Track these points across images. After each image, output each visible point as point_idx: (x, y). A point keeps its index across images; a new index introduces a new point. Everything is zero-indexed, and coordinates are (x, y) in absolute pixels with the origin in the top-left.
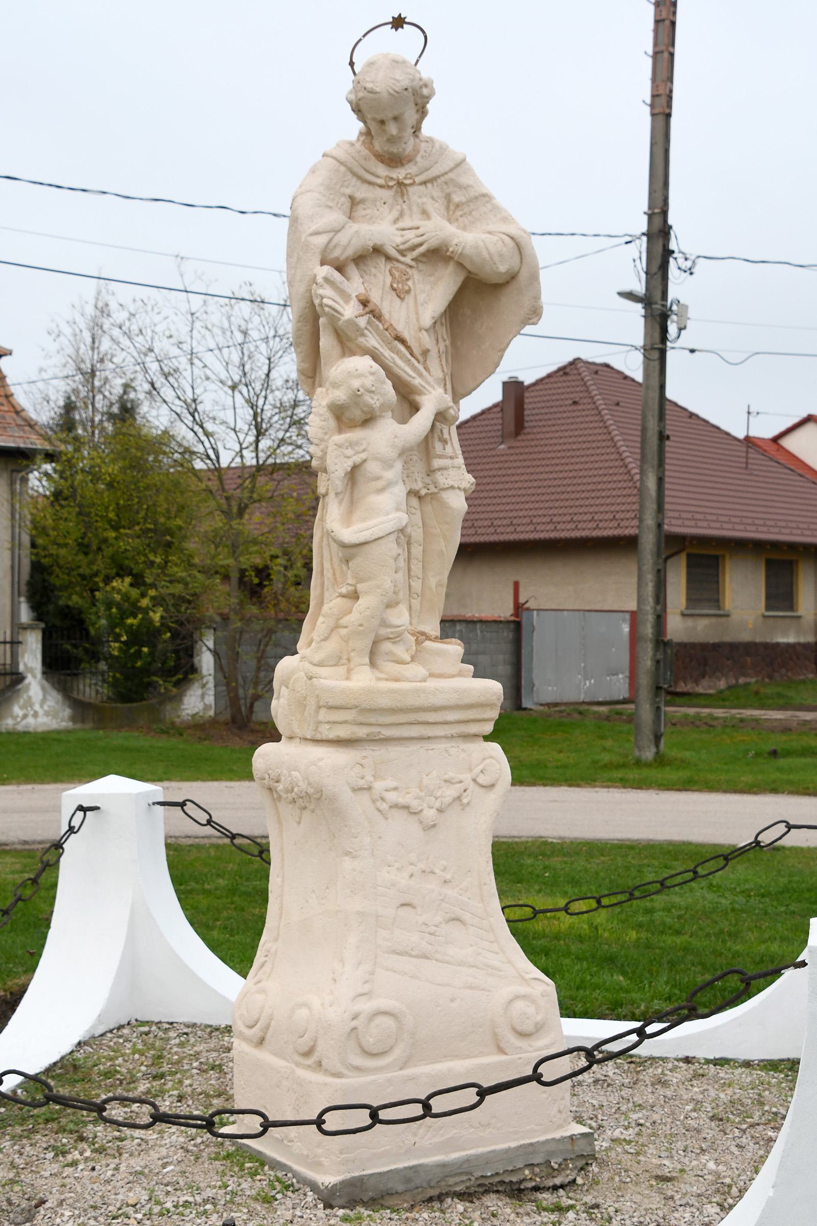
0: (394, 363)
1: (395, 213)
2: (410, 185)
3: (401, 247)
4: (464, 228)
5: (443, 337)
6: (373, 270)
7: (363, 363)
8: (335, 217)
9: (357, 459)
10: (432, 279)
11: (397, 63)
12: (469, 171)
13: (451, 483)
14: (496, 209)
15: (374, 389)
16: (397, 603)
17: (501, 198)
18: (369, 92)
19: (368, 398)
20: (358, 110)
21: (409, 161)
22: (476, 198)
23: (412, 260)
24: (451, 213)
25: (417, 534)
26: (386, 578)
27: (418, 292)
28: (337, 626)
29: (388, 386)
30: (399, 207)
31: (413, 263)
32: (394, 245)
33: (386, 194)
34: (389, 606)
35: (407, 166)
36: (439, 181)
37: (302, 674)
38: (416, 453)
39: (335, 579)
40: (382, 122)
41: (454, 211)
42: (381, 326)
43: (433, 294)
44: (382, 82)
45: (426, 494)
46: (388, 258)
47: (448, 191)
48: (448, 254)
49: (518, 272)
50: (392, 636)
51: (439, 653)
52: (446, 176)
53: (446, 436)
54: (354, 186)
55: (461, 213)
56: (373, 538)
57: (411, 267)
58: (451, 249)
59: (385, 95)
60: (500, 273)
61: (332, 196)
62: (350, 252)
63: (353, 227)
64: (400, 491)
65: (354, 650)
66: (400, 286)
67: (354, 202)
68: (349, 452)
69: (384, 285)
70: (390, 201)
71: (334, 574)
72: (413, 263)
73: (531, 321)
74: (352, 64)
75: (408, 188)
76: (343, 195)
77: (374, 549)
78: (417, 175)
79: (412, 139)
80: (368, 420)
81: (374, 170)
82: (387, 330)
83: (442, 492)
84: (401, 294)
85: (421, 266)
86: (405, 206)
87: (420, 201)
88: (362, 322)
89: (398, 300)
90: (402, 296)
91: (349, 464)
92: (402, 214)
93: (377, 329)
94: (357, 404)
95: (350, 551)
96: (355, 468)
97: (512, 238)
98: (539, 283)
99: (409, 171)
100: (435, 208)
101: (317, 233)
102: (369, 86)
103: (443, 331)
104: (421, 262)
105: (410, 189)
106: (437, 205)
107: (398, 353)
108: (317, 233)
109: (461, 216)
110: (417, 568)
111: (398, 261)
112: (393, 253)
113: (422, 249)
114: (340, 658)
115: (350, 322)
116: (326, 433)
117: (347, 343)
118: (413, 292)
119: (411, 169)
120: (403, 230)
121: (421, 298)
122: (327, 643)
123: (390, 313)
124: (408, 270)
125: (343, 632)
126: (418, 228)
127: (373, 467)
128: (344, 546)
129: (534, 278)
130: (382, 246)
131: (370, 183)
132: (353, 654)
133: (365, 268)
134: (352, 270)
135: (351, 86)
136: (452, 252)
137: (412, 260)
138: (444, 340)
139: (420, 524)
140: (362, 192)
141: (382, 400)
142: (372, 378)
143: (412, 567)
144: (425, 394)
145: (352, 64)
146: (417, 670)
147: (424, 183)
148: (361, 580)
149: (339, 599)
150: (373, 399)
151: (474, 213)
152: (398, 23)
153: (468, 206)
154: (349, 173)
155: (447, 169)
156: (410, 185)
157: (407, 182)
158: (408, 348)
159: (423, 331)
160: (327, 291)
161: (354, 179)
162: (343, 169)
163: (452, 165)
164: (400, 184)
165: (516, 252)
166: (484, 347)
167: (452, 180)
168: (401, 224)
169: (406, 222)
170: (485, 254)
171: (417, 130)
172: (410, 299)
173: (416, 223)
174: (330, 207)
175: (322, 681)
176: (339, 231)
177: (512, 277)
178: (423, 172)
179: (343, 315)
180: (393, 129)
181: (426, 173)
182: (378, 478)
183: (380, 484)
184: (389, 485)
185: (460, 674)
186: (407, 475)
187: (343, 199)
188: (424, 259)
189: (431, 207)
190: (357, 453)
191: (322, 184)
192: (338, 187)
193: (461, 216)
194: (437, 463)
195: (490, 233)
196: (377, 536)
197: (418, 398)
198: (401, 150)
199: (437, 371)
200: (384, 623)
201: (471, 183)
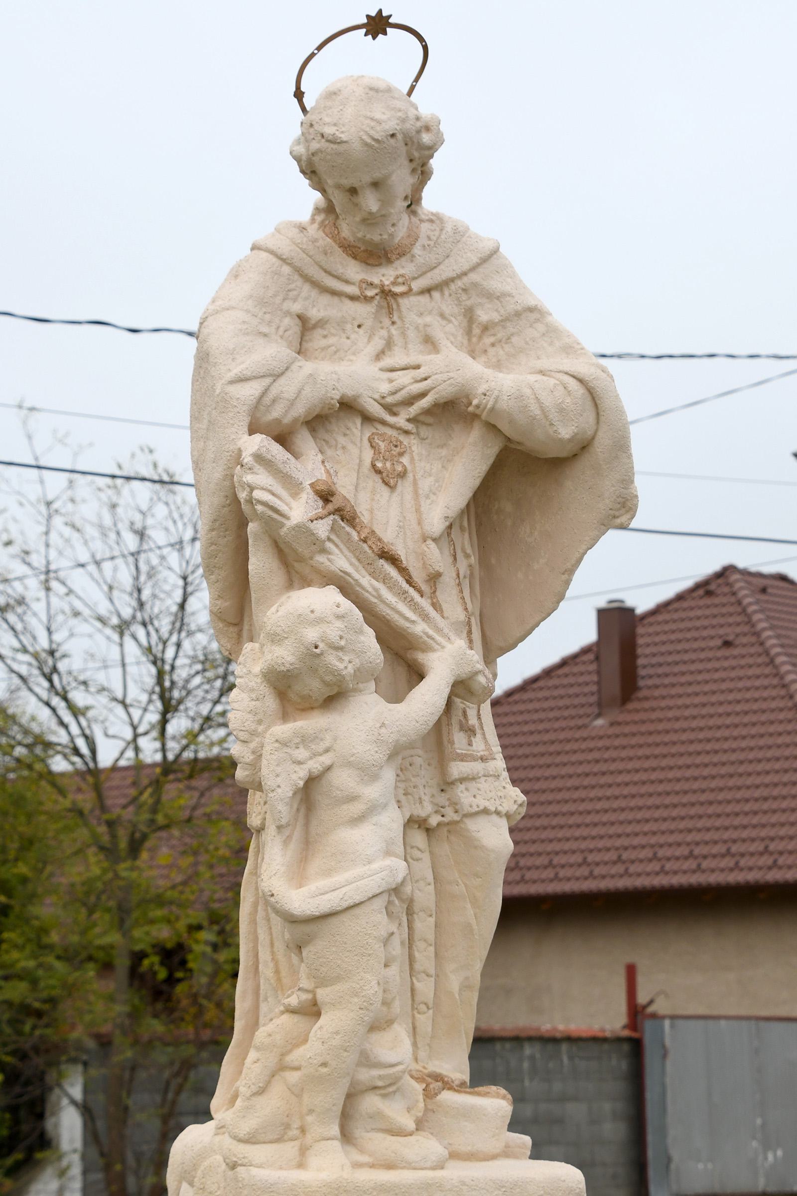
0: (379, 597)
1: (378, 343)
2: (403, 294)
3: (390, 400)
4: (498, 366)
5: (464, 550)
6: (342, 440)
7: (323, 599)
8: (272, 352)
9: (315, 765)
10: (444, 452)
11: (377, 92)
12: (505, 269)
13: (483, 803)
14: (553, 332)
15: (343, 643)
16: (390, 1022)
17: (563, 312)
18: (328, 141)
19: (331, 659)
20: (311, 170)
21: (402, 255)
22: (518, 314)
23: (409, 420)
24: (474, 340)
25: (425, 895)
26: (368, 976)
27: (418, 476)
28: (282, 1068)
29: (369, 638)
30: (384, 333)
31: (409, 427)
32: (377, 396)
33: (362, 311)
34: (375, 1027)
35: (397, 263)
36: (453, 286)
37: (219, 1158)
38: (420, 752)
39: (279, 980)
40: (353, 191)
41: (480, 338)
42: (354, 534)
43: (446, 478)
44: (351, 125)
45: (439, 824)
46: (367, 419)
47: (469, 303)
48: (471, 409)
49: (593, 438)
51: (466, 1113)
52: (465, 279)
53: (473, 721)
54: (306, 299)
55: (492, 339)
56: (345, 904)
57: (407, 432)
58: (475, 402)
59: (357, 146)
60: (561, 440)
61: (268, 317)
62: (300, 410)
63: (306, 367)
64: (391, 820)
65: (311, 1111)
66: (388, 464)
67: (306, 326)
68: (301, 753)
69: (360, 465)
70: (368, 323)
71: (277, 972)
72: (409, 427)
73: (618, 521)
74: (299, 95)
75: (400, 300)
76: (288, 313)
77: (347, 925)
78: (414, 278)
79: (405, 219)
80: (334, 697)
81: (340, 270)
82: (365, 541)
83: (466, 820)
84: (389, 479)
85: (424, 431)
86: (394, 331)
87: (420, 321)
88: (322, 529)
89: (385, 490)
90: (392, 482)
91: (299, 776)
92: (389, 344)
93: (348, 541)
94: (313, 670)
95: (304, 929)
96: (312, 782)
97: (581, 381)
98: (630, 456)
99: (401, 271)
100: (447, 333)
101: (242, 380)
102: (329, 130)
103: (465, 541)
104: (424, 423)
105: (404, 302)
106: (450, 328)
107: (386, 580)
108: (242, 380)
109: (493, 345)
110: (425, 957)
111: (384, 423)
112: (375, 410)
113: (425, 403)
114: (287, 1126)
115: (300, 529)
116: (260, 722)
117: (296, 566)
118: (410, 476)
119: (405, 268)
120: (392, 370)
121: (425, 485)
122: (260, 1101)
123: (371, 511)
124: (402, 438)
125: (293, 1077)
126: (418, 367)
127: (343, 780)
128: (292, 920)
129: (622, 446)
130: (356, 398)
131: (334, 293)
132: (309, 1119)
133: (327, 436)
134: (305, 441)
135: (297, 131)
136: (478, 407)
137: (409, 420)
138: (467, 556)
139: (430, 878)
140: (320, 308)
141: (357, 662)
142: (339, 624)
143: (417, 954)
144: (434, 650)
145: (299, 95)
146: (427, 1146)
147: (428, 291)
148: (323, 982)
149: (286, 1018)
150: (341, 660)
151: (514, 339)
152: (377, 25)
153: (504, 327)
154: (296, 277)
155: (466, 267)
156: (403, 294)
157: (398, 289)
158: (403, 571)
159: (429, 542)
160: (260, 478)
161: (307, 287)
162: (286, 269)
163: (475, 260)
164: (386, 293)
165: (589, 404)
166: (536, 566)
167: (475, 285)
168: (388, 362)
169: (398, 358)
170: (535, 410)
171: (413, 202)
172: (405, 487)
173: (413, 359)
174: (265, 335)
175: (254, 1171)
177: (582, 447)
178: (424, 273)
179: (288, 518)
180: (371, 202)
181: (429, 275)
182: (352, 798)
183: (356, 808)
184: (373, 809)
185: (507, 1153)
186: (404, 791)
187: (287, 321)
188: (429, 420)
189: (439, 330)
190: (315, 755)
191: (251, 296)
192: (278, 300)
193: (493, 345)
194: (457, 769)
195: (542, 372)
196: (350, 902)
197: (421, 657)
198: (385, 237)
199: (454, 610)
200: (366, 1060)
201: (508, 288)
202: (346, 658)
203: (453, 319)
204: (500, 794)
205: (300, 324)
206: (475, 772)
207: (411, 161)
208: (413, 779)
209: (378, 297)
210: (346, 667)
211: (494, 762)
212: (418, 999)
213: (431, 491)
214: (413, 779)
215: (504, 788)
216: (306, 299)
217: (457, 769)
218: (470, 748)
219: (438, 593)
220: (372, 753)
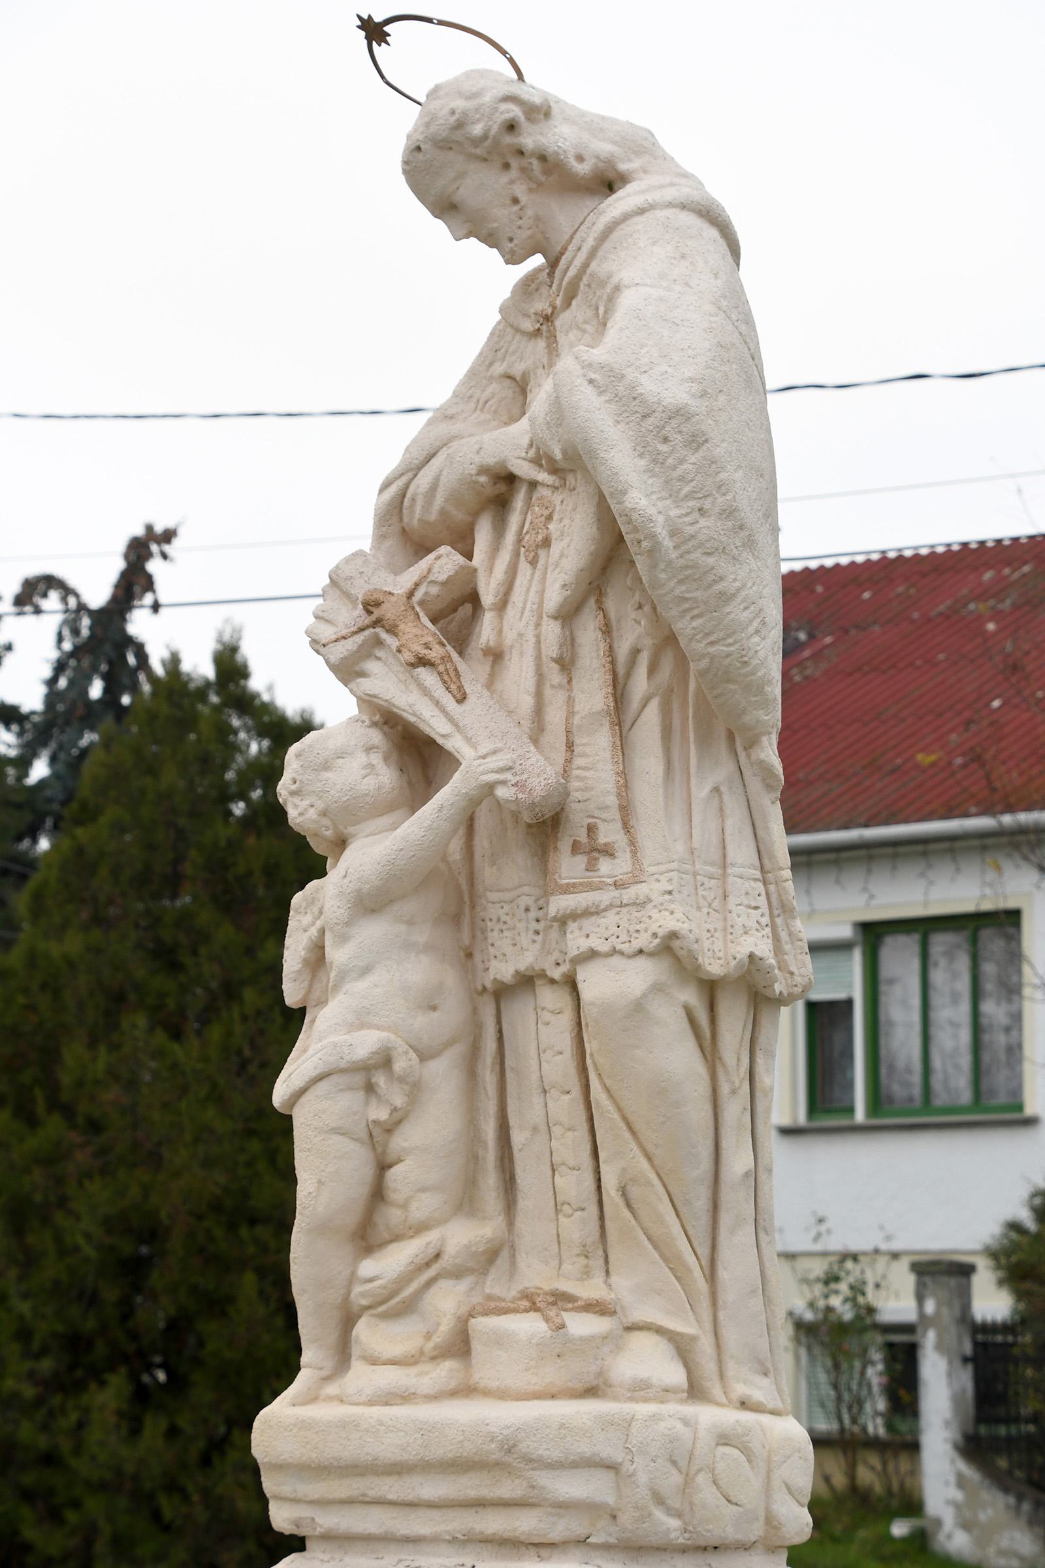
0: (415, 715)
32: (523, 454)
50: (364, 1302)
51: (500, 1340)
54: (514, 353)
76: (491, 379)
107: (425, 691)
141: (320, 805)
150: (296, 806)
161: (518, 337)
174: (452, 418)
176: (419, 468)
187: (490, 390)
202: (305, 803)
203: (587, 327)
204: (638, 927)
205: (514, 384)
206: (584, 905)
207: (486, 160)
208: (518, 925)
209: (544, 328)
210: (301, 814)
211: (639, 886)
212: (560, 1199)
213: (562, 555)
214: (518, 925)
215: (650, 917)
216: (514, 353)
217: (560, 904)
218: (588, 874)
219: (574, 682)
220: (335, 909)
